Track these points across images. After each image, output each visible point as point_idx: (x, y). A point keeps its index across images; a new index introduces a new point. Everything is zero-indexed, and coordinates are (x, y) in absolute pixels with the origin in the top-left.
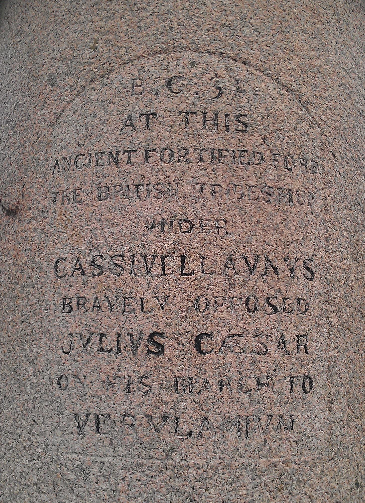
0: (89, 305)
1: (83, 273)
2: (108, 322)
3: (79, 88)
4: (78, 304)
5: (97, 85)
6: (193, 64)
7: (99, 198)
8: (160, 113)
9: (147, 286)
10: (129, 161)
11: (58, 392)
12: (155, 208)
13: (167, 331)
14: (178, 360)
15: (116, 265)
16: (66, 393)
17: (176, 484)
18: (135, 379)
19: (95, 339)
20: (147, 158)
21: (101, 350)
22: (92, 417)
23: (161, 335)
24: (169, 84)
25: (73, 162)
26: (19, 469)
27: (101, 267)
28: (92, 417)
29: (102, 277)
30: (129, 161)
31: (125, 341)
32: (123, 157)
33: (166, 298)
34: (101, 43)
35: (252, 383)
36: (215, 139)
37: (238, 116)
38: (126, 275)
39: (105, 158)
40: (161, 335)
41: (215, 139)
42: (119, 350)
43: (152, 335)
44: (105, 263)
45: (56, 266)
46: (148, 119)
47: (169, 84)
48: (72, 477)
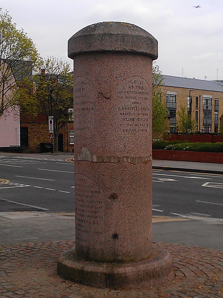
0: (125, 114)
1: (124, 109)
2: (127, 116)
3: (122, 80)
4: (123, 114)
5: (125, 80)
6: (138, 79)
7: (126, 98)
8: (134, 86)
9: (132, 112)
10: (130, 93)
11: (120, 127)
12: (133, 100)
13: (135, 118)
14: (136, 122)
15: (128, 108)
16: (121, 127)
17: (136, 138)
18: (131, 124)
19: (126, 119)
20: (132, 93)
21: (126, 120)
22: (125, 130)
23: (134, 118)
24: (135, 82)
25: (121, 92)
26: (113, 139)
27: (126, 109)
28: (125, 130)
29: (126, 110)
30: (130, 93)
31: (130, 119)
32: (129, 92)
33: (135, 113)
34: (125, 73)
35: (143, 125)
36: (140, 91)
37: (142, 87)
38: (130, 110)
39: (127, 92)
40: (134, 118)
41: (140, 91)
42: (129, 121)
43: (133, 118)
44: (127, 108)
45: (119, 108)
46: (132, 87)
47: (135, 82)
48: (123, 138)
